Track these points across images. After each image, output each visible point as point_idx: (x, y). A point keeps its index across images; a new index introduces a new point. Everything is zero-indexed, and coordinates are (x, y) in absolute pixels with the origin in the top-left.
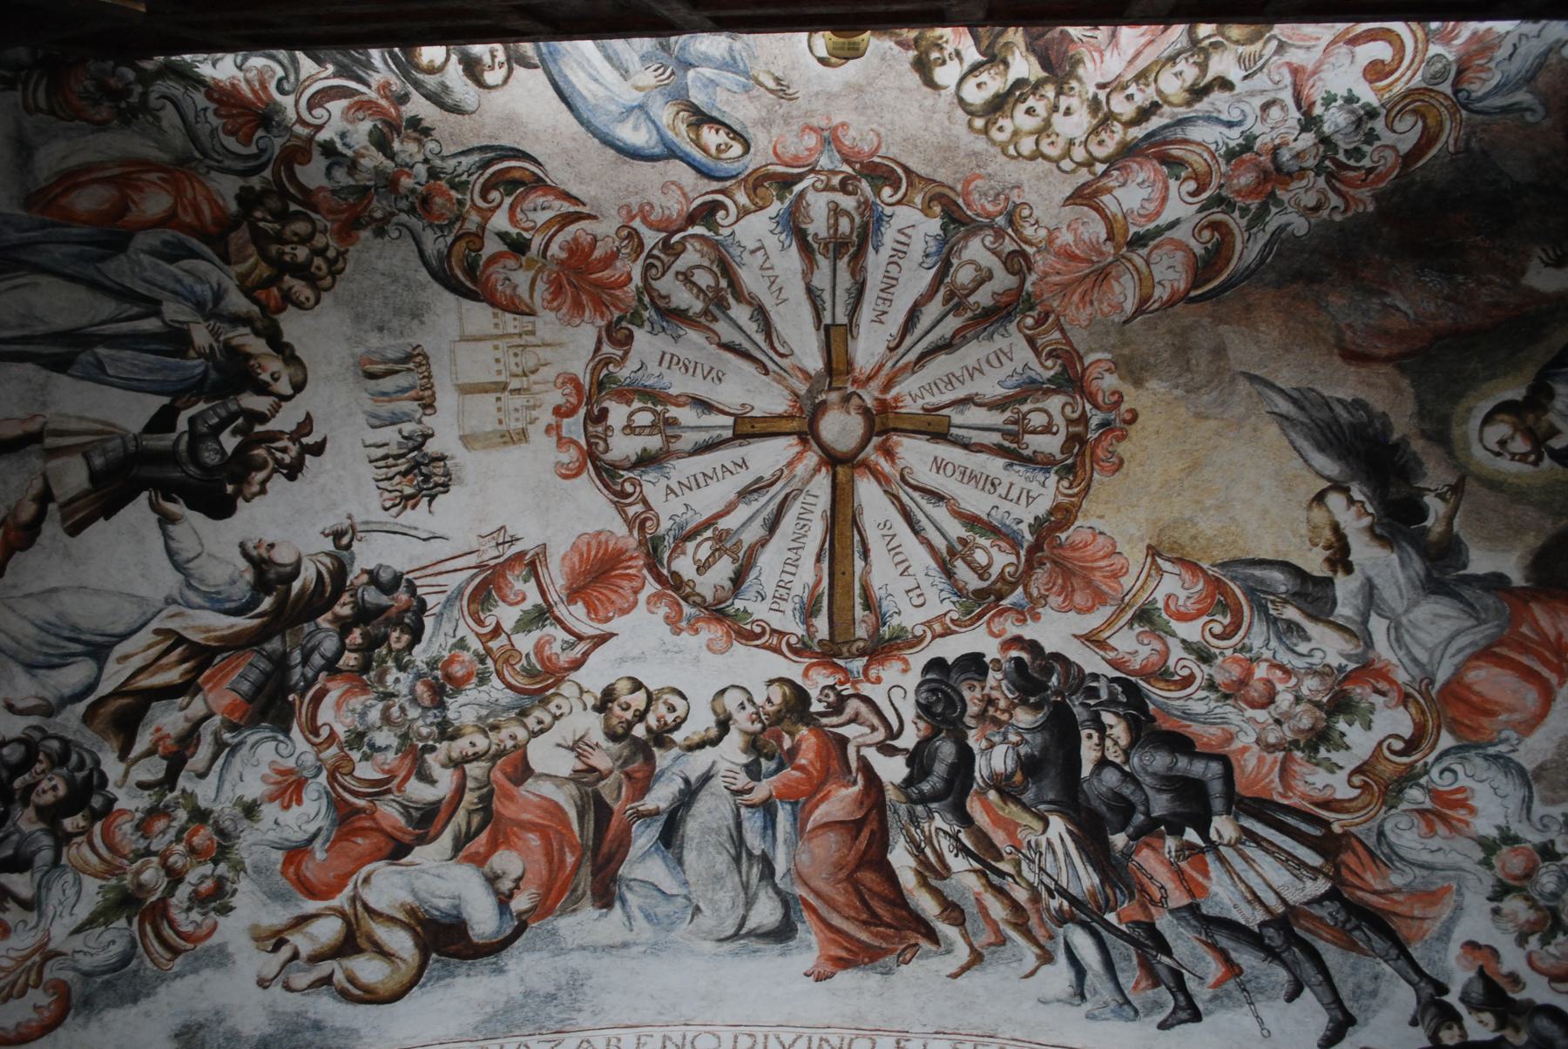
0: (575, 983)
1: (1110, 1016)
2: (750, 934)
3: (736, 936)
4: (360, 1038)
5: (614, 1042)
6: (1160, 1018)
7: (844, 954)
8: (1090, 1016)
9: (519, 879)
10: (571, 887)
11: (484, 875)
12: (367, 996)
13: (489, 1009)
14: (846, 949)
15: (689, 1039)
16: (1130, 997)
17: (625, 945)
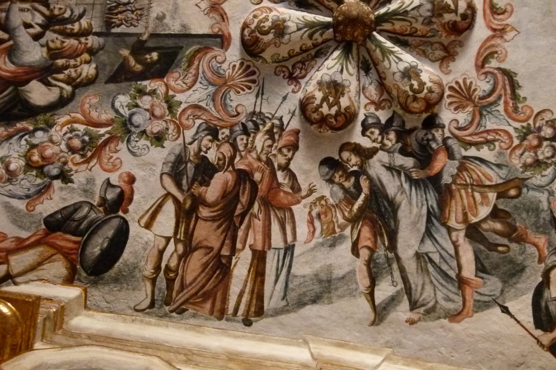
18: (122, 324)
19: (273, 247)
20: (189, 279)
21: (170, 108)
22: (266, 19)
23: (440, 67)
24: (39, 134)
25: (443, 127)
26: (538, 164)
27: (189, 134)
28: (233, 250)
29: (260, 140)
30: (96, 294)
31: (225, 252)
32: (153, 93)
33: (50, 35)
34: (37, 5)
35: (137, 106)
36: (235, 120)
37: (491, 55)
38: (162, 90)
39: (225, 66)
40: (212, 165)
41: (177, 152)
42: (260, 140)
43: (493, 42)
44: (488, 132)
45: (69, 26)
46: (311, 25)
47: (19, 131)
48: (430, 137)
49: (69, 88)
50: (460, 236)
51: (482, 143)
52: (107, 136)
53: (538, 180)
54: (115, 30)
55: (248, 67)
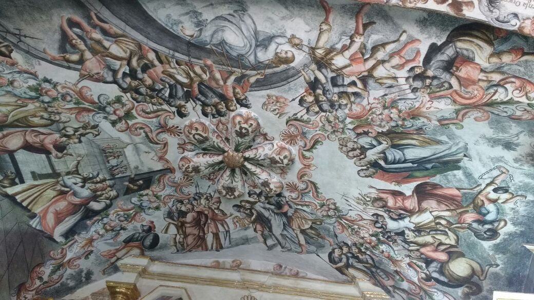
18: (168, 267)
19: (221, 231)
20: (189, 243)
21: (157, 198)
23: (281, 176)
25: (285, 197)
26: (329, 216)
27: (170, 204)
28: (204, 234)
29: (203, 201)
30: (155, 253)
31: (201, 234)
32: (147, 195)
33: (87, 185)
34: (75, 175)
35: (142, 200)
36: (189, 197)
37: (305, 175)
38: (151, 193)
39: (176, 179)
40: (185, 212)
41: (168, 210)
42: (203, 201)
43: (305, 170)
44: (306, 202)
45: (95, 180)
46: (212, 165)
48: (280, 200)
49: (108, 202)
51: (304, 205)
52: (134, 213)
53: (328, 221)
54: (117, 176)
55: (187, 178)
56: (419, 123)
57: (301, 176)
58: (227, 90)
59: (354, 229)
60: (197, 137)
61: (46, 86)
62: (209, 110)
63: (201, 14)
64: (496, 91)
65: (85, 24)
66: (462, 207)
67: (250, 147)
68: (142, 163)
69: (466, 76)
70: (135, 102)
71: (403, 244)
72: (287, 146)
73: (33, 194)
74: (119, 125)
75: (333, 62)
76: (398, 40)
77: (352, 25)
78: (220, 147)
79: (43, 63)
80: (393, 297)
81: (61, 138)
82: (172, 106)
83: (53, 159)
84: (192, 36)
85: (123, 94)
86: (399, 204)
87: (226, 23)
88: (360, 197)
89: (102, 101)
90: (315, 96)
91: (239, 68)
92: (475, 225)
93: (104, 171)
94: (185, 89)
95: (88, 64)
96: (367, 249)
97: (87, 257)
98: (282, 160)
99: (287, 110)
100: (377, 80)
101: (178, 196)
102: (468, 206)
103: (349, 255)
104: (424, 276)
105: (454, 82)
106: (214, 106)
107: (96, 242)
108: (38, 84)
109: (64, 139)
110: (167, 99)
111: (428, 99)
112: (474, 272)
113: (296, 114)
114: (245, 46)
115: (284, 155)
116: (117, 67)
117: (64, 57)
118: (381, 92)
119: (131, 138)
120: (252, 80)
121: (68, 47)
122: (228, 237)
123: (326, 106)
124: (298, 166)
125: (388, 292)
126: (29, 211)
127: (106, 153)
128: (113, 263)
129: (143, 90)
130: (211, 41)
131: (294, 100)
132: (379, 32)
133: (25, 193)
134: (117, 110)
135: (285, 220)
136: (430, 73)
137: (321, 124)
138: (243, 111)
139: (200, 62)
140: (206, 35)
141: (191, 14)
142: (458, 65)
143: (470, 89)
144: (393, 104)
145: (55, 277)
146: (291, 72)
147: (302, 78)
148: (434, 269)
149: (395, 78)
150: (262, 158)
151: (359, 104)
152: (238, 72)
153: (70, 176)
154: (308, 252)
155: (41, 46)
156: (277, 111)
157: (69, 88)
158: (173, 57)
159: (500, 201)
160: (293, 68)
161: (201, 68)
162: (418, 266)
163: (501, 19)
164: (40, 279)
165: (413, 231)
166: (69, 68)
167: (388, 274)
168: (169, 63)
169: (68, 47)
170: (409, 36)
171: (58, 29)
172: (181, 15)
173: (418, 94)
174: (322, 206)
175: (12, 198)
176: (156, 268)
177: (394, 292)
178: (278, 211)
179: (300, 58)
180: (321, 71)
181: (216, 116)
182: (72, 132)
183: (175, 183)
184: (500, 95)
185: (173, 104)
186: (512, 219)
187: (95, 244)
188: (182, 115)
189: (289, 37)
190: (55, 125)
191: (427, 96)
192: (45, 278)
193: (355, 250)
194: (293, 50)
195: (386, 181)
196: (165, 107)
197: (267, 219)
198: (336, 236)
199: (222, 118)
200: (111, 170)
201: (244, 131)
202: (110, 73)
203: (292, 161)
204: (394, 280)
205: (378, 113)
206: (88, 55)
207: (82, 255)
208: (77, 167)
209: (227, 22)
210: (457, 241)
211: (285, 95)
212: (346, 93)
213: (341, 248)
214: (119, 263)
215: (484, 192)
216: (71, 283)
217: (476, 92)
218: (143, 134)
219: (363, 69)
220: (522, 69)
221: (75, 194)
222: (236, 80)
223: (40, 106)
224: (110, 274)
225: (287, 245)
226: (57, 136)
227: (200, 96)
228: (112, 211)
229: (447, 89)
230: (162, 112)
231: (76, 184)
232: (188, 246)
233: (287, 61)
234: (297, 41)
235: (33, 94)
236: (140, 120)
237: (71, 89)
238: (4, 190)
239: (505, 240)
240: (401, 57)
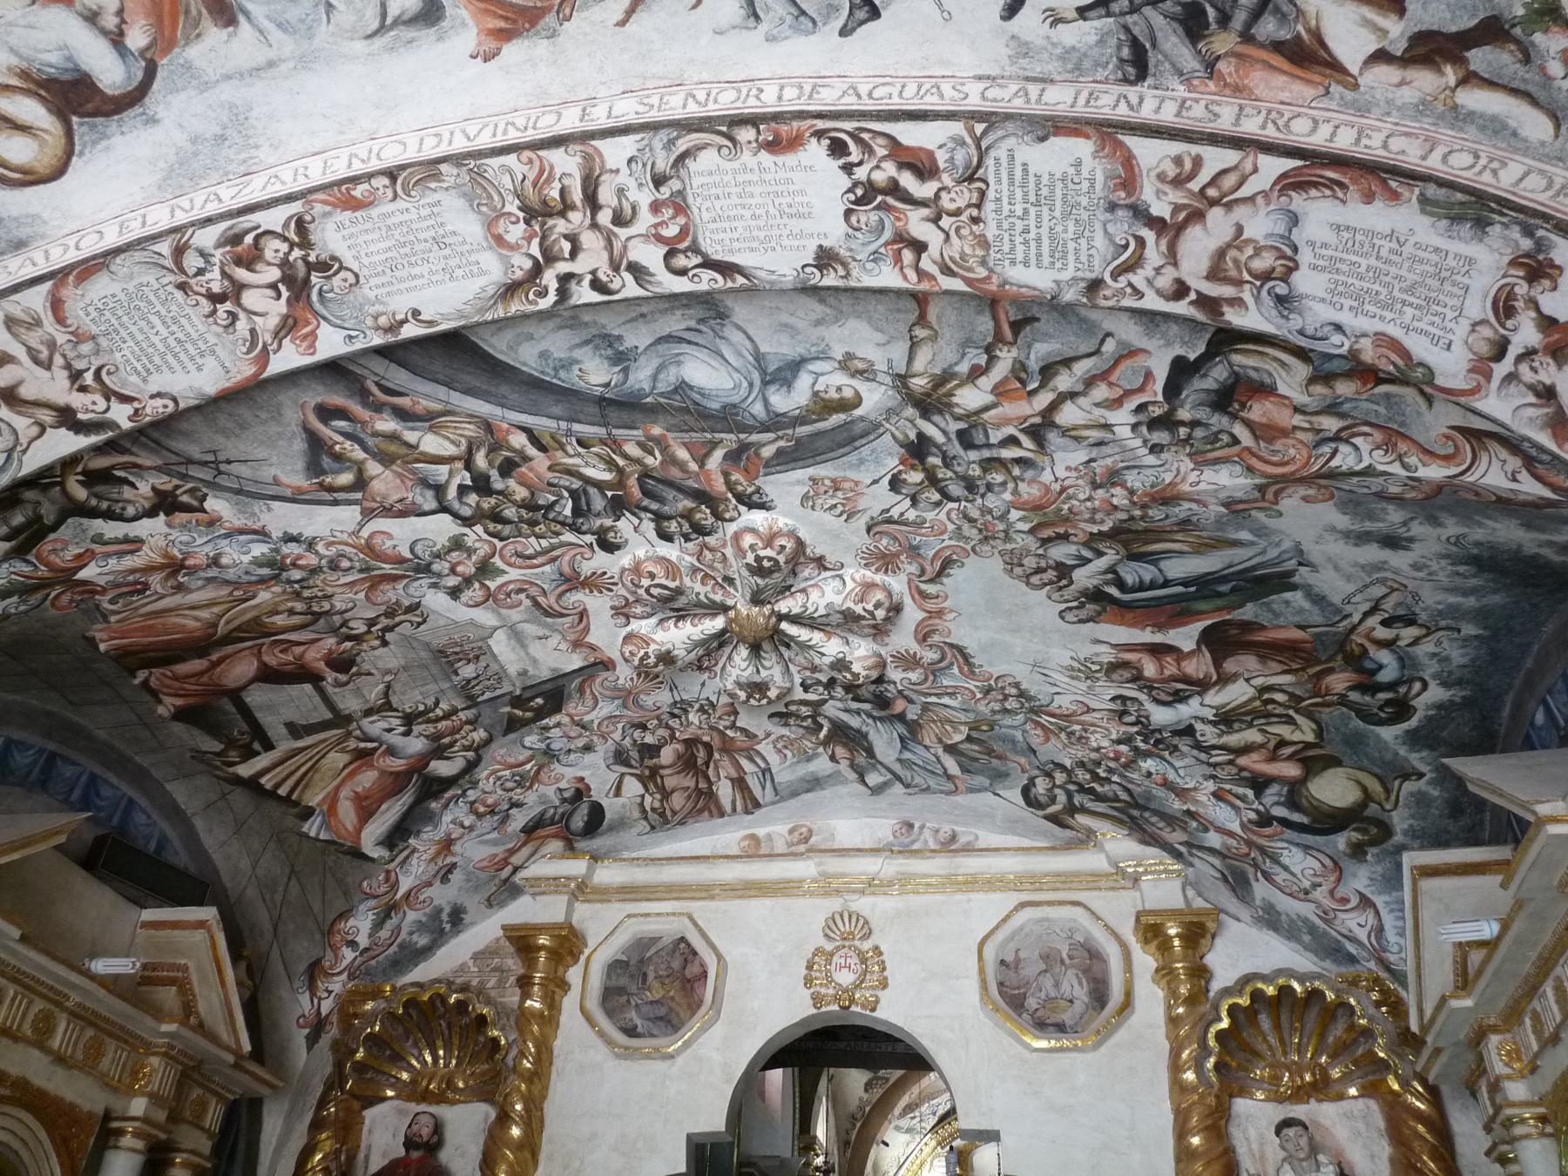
0: (238, 117)
1: (789, 32)
2: (397, 22)
3: (382, 29)
4: (45, 222)
5: (301, 171)
6: (839, 23)
7: (502, 24)
8: (770, 39)
9: (120, 12)
10: (182, 9)
11: (80, 14)
12: (30, 178)
13: (162, 165)
14: (502, 17)
15: (375, 151)
16: (804, 6)
17: (271, 64)
21: (583, 727)
22: (646, 654)
24: (470, 792)
26: (1006, 711)
27: (617, 736)
28: (710, 783)
29: (693, 717)
30: (597, 843)
32: (558, 725)
33: (416, 729)
37: (934, 631)
39: (621, 681)
42: (693, 717)
47: (450, 800)
49: (470, 754)
50: (940, 751)
53: (1008, 721)
56: (1182, 510)
57: (923, 636)
58: (709, 480)
59: (1073, 733)
60: (655, 591)
61: (292, 549)
62: (673, 526)
63: (619, 338)
64: (1335, 452)
65: (356, 408)
66: (1319, 662)
67: (789, 588)
68: (535, 661)
69: (1264, 420)
70: (495, 541)
71: (1195, 752)
72: (879, 578)
73: (299, 768)
74: (466, 596)
75: (955, 400)
76: (1097, 352)
77: (985, 324)
78: (714, 602)
79: (275, 504)
80: (1192, 865)
81: (339, 643)
82: (584, 533)
83: (330, 690)
84: (607, 385)
85: (466, 530)
86: (1171, 669)
87: (685, 348)
88: (1076, 665)
89: (420, 553)
90: (925, 470)
91: (731, 432)
92: (1354, 696)
93: (450, 694)
94: (609, 494)
95: (377, 486)
96: (1110, 771)
97: (445, 880)
98: (871, 613)
99: (862, 503)
100: (1065, 432)
101: (633, 714)
102: (1331, 659)
103: (1072, 787)
104: (1253, 816)
105: (1239, 430)
106: (682, 516)
107: (459, 843)
108: (272, 550)
109: (348, 644)
110: (569, 521)
111: (1191, 466)
112: (1367, 796)
113: (888, 511)
114: (737, 386)
115: (874, 601)
116: (443, 479)
117: (321, 484)
118: (1081, 456)
119: (499, 614)
120: (768, 452)
121: (326, 461)
122: (768, 784)
123: (955, 489)
124: (912, 614)
125: (1178, 856)
126: (296, 804)
127: (446, 658)
128: (507, 879)
129: (510, 512)
130: (654, 388)
131: (875, 482)
132: (1051, 337)
133: (278, 769)
134: (459, 563)
135: (902, 729)
136: (1184, 414)
137: (951, 527)
138: (757, 518)
139: (635, 432)
140: (641, 377)
141: (598, 341)
142: (1244, 399)
143: (1278, 445)
144: (1113, 478)
145: (384, 934)
146: (861, 426)
147: (888, 436)
148: (1276, 798)
149: (1107, 427)
150: (822, 611)
151: (1032, 481)
152: (730, 440)
153: (375, 718)
154: (971, 790)
155: (267, 473)
156: (840, 508)
157: (340, 543)
158: (569, 434)
159: (1402, 643)
160: (862, 419)
161: (640, 444)
162: (1237, 797)
163: (1310, 331)
164: (352, 944)
165: (1214, 723)
166: (336, 503)
167: (1170, 820)
168: (562, 447)
169: (326, 461)
170: (1121, 343)
171: (298, 430)
172: (571, 348)
173: (1164, 456)
174: (987, 691)
175: (252, 784)
176: (607, 874)
177: (1192, 855)
178: (883, 713)
179: (874, 398)
180: (929, 420)
181: (694, 536)
182: (363, 629)
183: (620, 690)
184: (1345, 459)
185: (584, 528)
186: (1435, 676)
187: (457, 848)
188: (609, 547)
189: (840, 357)
190: (322, 621)
191: (1187, 460)
192: (363, 941)
193: (1082, 776)
194: (854, 382)
195: (1130, 626)
196: (569, 537)
197: (858, 731)
198: (1034, 752)
199: (707, 539)
200: (467, 691)
201: (766, 564)
202: (430, 494)
203: (896, 609)
204: (1185, 830)
205: (1082, 496)
206: (373, 468)
207: (435, 876)
208: (386, 695)
209: (684, 345)
210: (1320, 732)
211: (851, 475)
212: (999, 460)
213: (1049, 775)
214: (517, 878)
215: (1361, 629)
216: (422, 941)
217: (1292, 452)
218: (527, 602)
219: (1028, 411)
220: (1382, 410)
221: (392, 751)
222: (726, 457)
223: (284, 592)
224: (502, 904)
225: (917, 780)
226: (331, 642)
227: (646, 502)
228: (482, 773)
229: (1228, 445)
230: (564, 549)
231: (389, 730)
232: (674, 813)
233: (844, 406)
234: (861, 365)
235: (266, 571)
236: (514, 574)
237: (347, 544)
238: (231, 770)
239: (1429, 719)
240: (1111, 384)
